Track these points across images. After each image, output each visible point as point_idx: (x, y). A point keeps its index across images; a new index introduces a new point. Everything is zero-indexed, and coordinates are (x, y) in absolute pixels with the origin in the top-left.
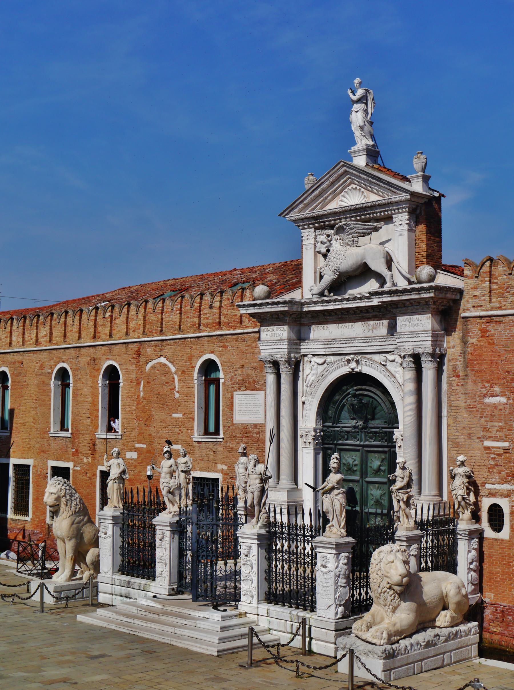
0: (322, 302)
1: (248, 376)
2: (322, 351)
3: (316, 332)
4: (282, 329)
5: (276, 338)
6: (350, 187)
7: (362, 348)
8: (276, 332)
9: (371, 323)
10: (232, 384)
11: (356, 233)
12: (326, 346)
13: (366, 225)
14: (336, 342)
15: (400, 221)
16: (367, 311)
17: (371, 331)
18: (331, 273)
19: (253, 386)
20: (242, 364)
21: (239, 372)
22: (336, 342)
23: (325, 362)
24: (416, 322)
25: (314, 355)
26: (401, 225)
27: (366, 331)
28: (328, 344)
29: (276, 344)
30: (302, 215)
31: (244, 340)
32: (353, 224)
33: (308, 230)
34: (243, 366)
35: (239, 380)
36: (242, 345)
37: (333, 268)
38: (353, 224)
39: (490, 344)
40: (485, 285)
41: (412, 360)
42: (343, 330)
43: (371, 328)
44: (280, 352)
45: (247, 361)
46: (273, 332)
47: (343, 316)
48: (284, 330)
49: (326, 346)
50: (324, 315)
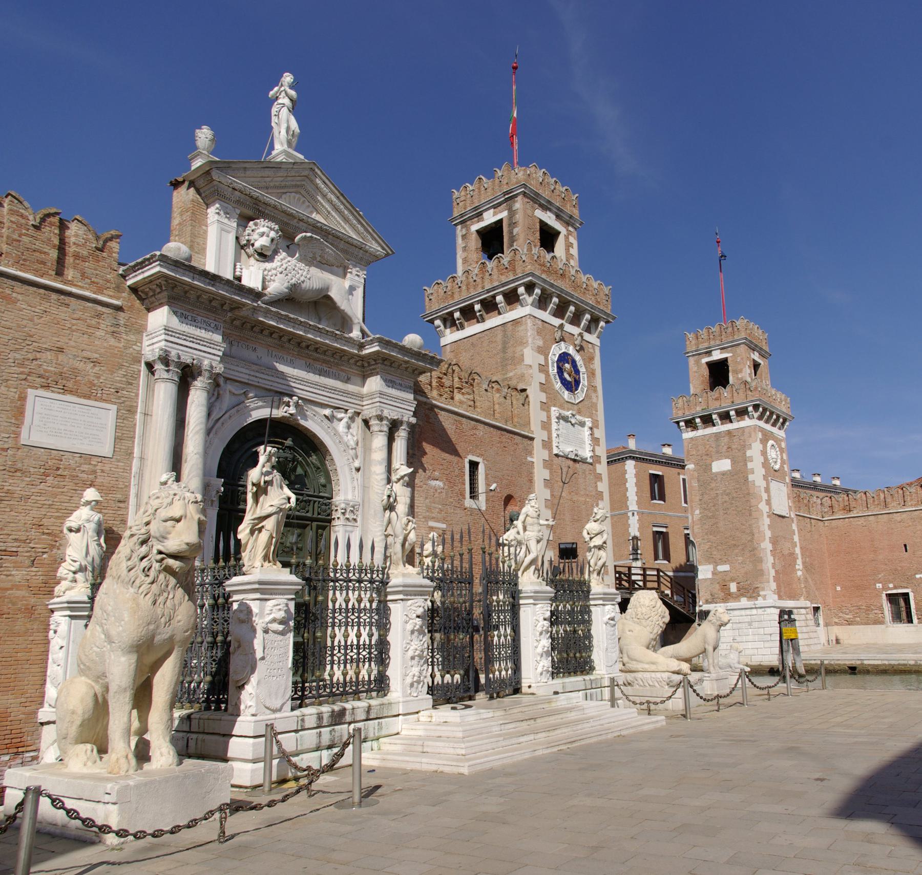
1: (75, 372)
2: (244, 378)
3: (234, 348)
4: (212, 325)
9: (318, 366)
10: (22, 373)
12: (252, 373)
16: (325, 352)
19: (85, 389)
20: (59, 344)
21: (49, 355)
31: (67, 305)
34: (61, 350)
35: (46, 371)
36: (63, 313)
37: (293, 281)
45: (72, 343)
47: (287, 345)
49: (252, 373)
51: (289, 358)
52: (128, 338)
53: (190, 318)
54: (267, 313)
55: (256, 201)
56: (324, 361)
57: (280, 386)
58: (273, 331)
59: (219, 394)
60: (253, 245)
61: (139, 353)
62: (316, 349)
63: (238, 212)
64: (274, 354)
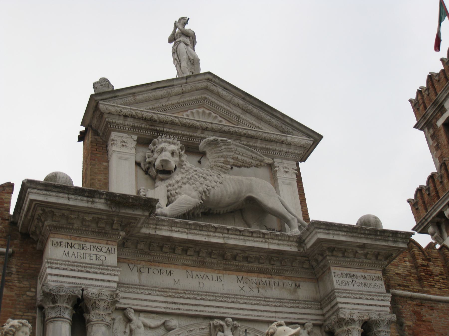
0: (189, 227)
3: (144, 276)
4: (104, 250)
5: (88, 260)
6: (201, 110)
7: (241, 312)
8: (88, 252)
9: (254, 278)
11: (233, 158)
12: (169, 300)
13: (254, 153)
14: (192, 296)
15: (286, 168)
17: (256, 290)
18: (195, 194)
22: (192, 296)
23: (164, 324)
24: (363, 281)
25: (138, 312)
26: (286, 172)
27: (246, 289)
28: (175, 297)
29: (92, 270)
30: (128, 110)
32: (235, 145)
33: (125, 135)
37: (201, 189)
38: (235, 145)
39: (429, 330)
40: (405, 264)
41: (360, 328)
42: (201, 280)
43: (254, 285)
44: (97, 285)
46: (82, 251)
47: (208, 260)
48: (109, 251)
49: (169, 300)
50: (173, 250)
51: (215, 276)
52: (22, 285)
53: (76, 246)
54: (172, 224)
55: (151, 121)
56: (260, 272)
57: (207, 309)
58: (186, 247)
59: (131, 331)
60: (154, 165)
61: (34, 298)
62: (246, 259)
63: (135, 137)
64: (194, 274)
